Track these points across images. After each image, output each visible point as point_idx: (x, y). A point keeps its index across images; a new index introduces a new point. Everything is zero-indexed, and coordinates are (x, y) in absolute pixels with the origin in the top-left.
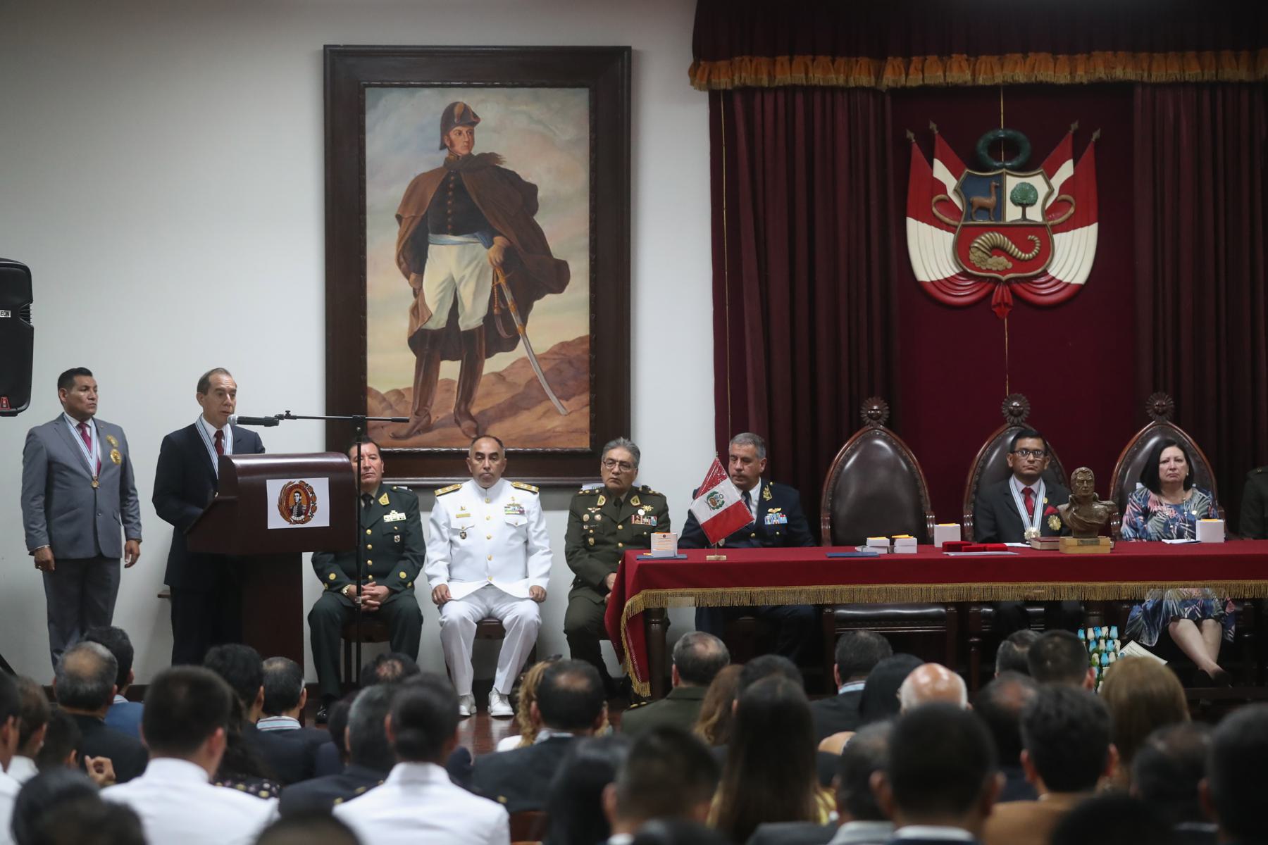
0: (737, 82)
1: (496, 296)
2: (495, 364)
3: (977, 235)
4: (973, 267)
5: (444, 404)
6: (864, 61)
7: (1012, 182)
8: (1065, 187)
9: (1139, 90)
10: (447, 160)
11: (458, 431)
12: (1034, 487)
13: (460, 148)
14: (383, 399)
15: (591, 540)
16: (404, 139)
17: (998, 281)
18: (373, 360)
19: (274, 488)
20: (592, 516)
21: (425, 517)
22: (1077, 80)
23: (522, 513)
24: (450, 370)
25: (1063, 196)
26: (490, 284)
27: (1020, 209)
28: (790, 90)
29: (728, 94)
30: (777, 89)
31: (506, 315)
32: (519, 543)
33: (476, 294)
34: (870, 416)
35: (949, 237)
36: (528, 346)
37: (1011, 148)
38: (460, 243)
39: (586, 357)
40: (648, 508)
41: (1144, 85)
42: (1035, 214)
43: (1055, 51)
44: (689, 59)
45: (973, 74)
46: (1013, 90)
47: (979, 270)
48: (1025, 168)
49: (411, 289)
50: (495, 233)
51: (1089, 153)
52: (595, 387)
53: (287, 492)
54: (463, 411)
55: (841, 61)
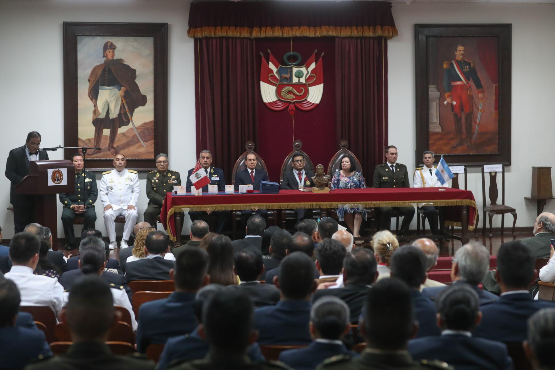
0: (203, 35)
1: (122, 107)
2: (122, 130)
3: (284, 87)
4: (282, 98)
5: (104, 144)
6: (246, 28)
7: (295, 70)
8: (313, 71)
9: (337, 40)
10: (105, 61)
11: (109, 152)
12: (301, 172)
13: (110, 57)
14: (84, 142)
15: (155, 189)
16: (90, 53)
17: (290, 102)
18: (80, 129)
19: (50, 172)
20: (155, 180)
21: (97, 181)
22: (317, 36)
23: (131, 181)
24: (106, 132)
26: (120, 103)
28: (221, 38)
29: (200, 40)
30: (217, 38)
31: (125, 113)
32: (130, 191)
33: (115, 107)
34: (248, 148)
35: (274, 88)
36: (133, 124)
37: (295, 58)
39: (153, 128)
40: (174, 177)
41: (338, 37)
43: (309, 26)
44: (187, 28)
45: (282, 34)
46: (295, 39)
48: (299, 65)
49: (93, 105)
50: (122, 86)
51: (320, 60)
52: (156, 138)
53: (54, 173)
54: (111, 146)
55: (238, 29)
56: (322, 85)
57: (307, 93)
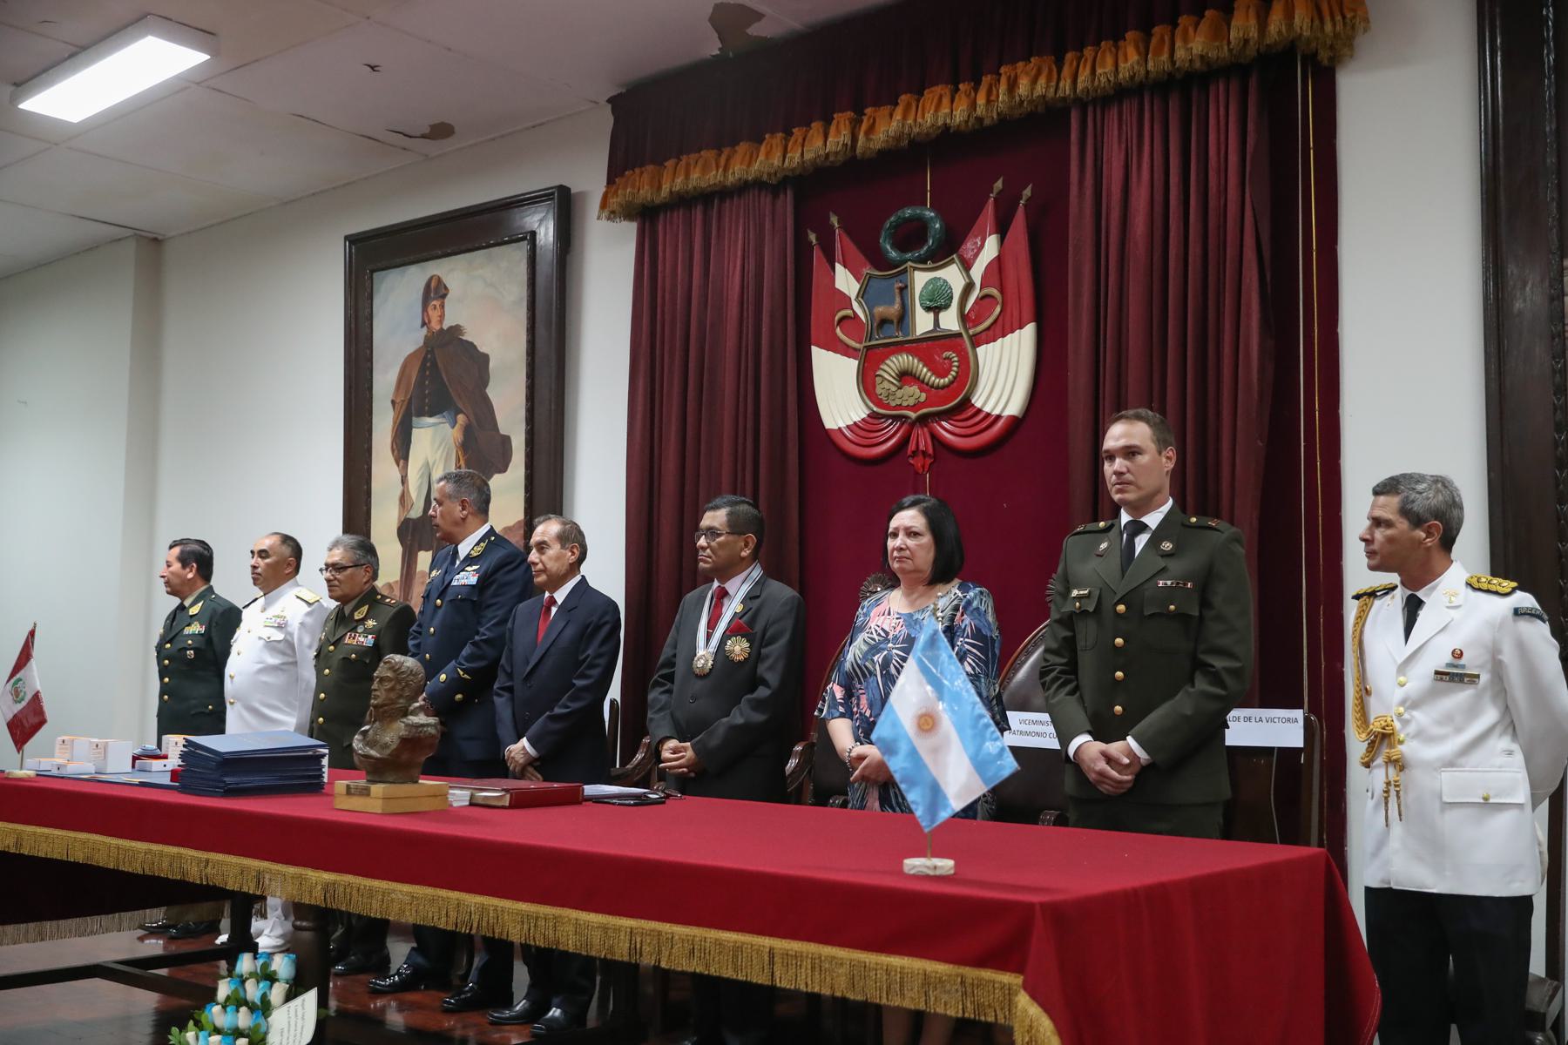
7: (921, 279)
13: (435, 326)
25: (986, 291)
27: (931, 315)
38: (434, 425)
42: (950, 321)
47: (887, 407)
50: (458, 411)
56: (1029, 330)
57: (968, 375)
